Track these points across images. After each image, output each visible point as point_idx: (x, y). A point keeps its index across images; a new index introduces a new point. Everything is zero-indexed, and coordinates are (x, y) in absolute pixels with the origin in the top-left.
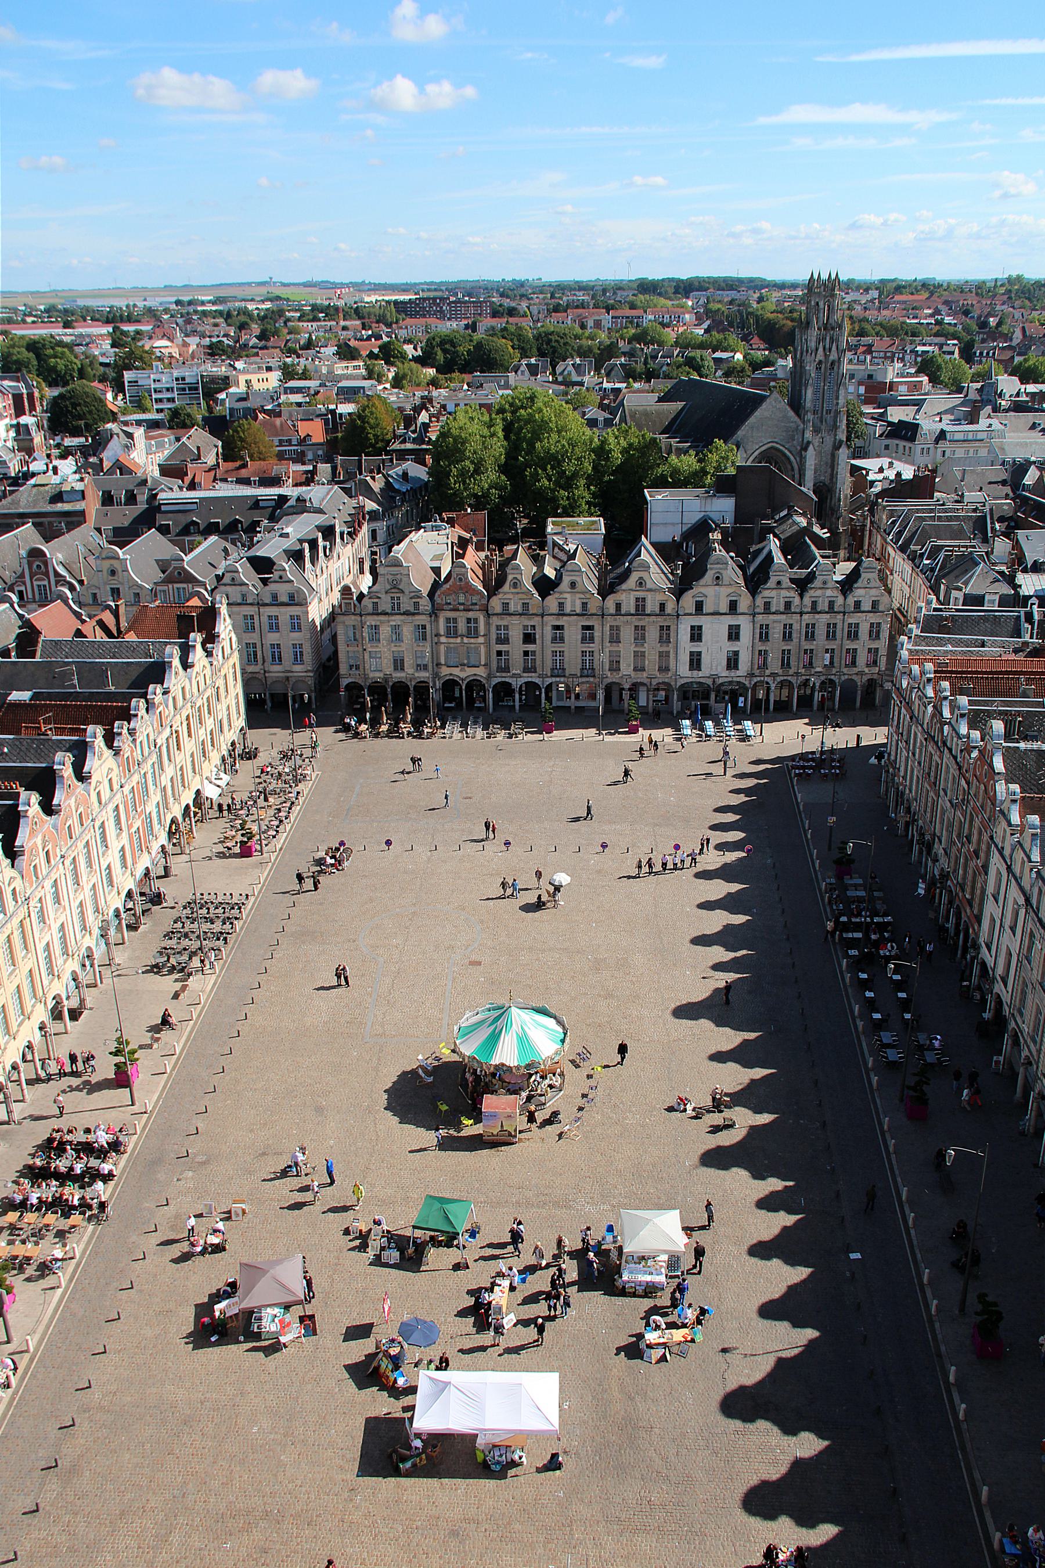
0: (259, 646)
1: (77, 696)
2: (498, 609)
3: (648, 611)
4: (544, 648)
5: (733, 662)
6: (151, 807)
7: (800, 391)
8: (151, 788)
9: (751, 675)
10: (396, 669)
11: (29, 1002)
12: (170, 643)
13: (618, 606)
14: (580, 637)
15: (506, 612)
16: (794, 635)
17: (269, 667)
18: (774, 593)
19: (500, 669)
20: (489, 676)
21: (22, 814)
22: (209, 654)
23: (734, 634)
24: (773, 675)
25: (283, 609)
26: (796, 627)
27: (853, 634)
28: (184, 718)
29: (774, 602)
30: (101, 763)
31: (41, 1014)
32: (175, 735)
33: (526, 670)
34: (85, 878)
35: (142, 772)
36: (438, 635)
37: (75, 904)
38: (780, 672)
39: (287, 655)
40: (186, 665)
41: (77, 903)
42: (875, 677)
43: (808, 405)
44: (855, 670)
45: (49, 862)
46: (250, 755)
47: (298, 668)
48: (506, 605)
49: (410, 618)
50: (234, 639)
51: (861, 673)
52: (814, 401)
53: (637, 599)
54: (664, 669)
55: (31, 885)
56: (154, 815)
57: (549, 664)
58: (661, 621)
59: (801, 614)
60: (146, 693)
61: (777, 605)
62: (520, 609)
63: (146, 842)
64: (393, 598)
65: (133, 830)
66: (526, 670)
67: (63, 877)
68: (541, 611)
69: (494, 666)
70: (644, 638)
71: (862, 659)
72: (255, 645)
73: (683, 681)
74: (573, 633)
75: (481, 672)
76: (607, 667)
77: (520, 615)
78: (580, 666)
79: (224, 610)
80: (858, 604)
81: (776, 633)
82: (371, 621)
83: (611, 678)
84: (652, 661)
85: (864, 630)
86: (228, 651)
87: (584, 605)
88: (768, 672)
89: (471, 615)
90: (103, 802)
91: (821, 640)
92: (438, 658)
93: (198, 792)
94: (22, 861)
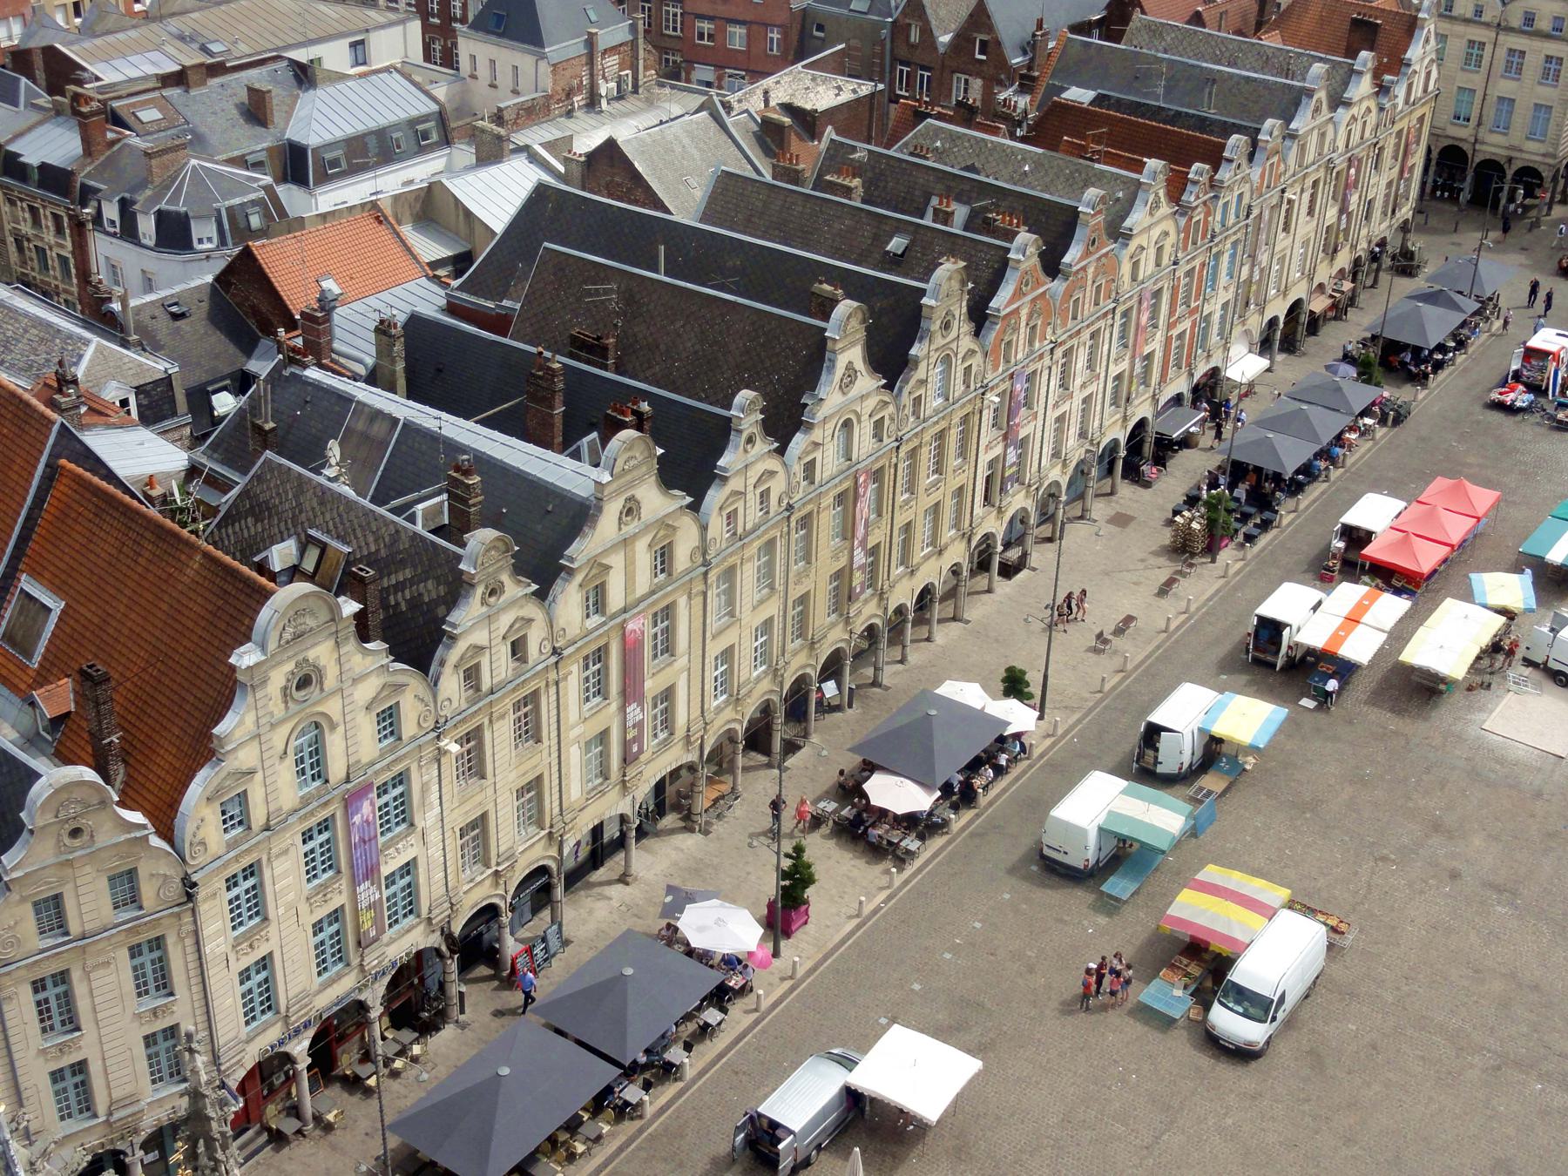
0: (1479, 94)
1: (1155, 113)
6: (1214, 308)
8: (1223, 279)
11: (948, 534)
12: (1321, 60)
17: (1483, 134)
21: (1011, 263)
22: (1382, 90)
25: (1537, 44)
28: (1309, 182)
30: (1152, 222)
31: (958, 553)
32: (1285, 207)
34: (1078, 382)
35: (1214, 250)
37: (1052, 415)
40: (1338, 101)
41: (1058, 413)
45: (1031, 343)
46: (1406, 265)
47: (1531, 146)
50: (1434, 75)
55: (995, 368)
56: (1216, 318)
60: (1258, 131)
63: (1189, 356)
65: (1175, 332)
67: (1046, 373)
79: (1430, 27)
86: (1417, 91)
90: (1141, 277)
93: (1296, 306)
94: (991, 335)
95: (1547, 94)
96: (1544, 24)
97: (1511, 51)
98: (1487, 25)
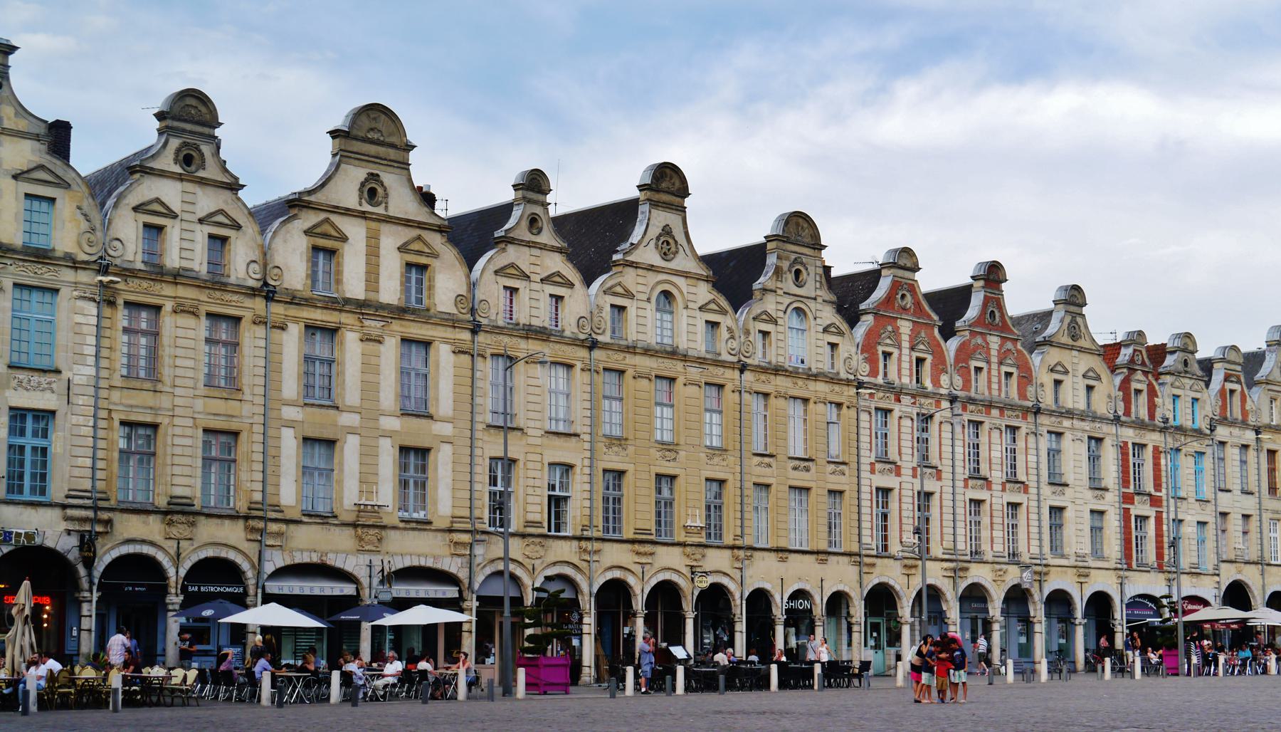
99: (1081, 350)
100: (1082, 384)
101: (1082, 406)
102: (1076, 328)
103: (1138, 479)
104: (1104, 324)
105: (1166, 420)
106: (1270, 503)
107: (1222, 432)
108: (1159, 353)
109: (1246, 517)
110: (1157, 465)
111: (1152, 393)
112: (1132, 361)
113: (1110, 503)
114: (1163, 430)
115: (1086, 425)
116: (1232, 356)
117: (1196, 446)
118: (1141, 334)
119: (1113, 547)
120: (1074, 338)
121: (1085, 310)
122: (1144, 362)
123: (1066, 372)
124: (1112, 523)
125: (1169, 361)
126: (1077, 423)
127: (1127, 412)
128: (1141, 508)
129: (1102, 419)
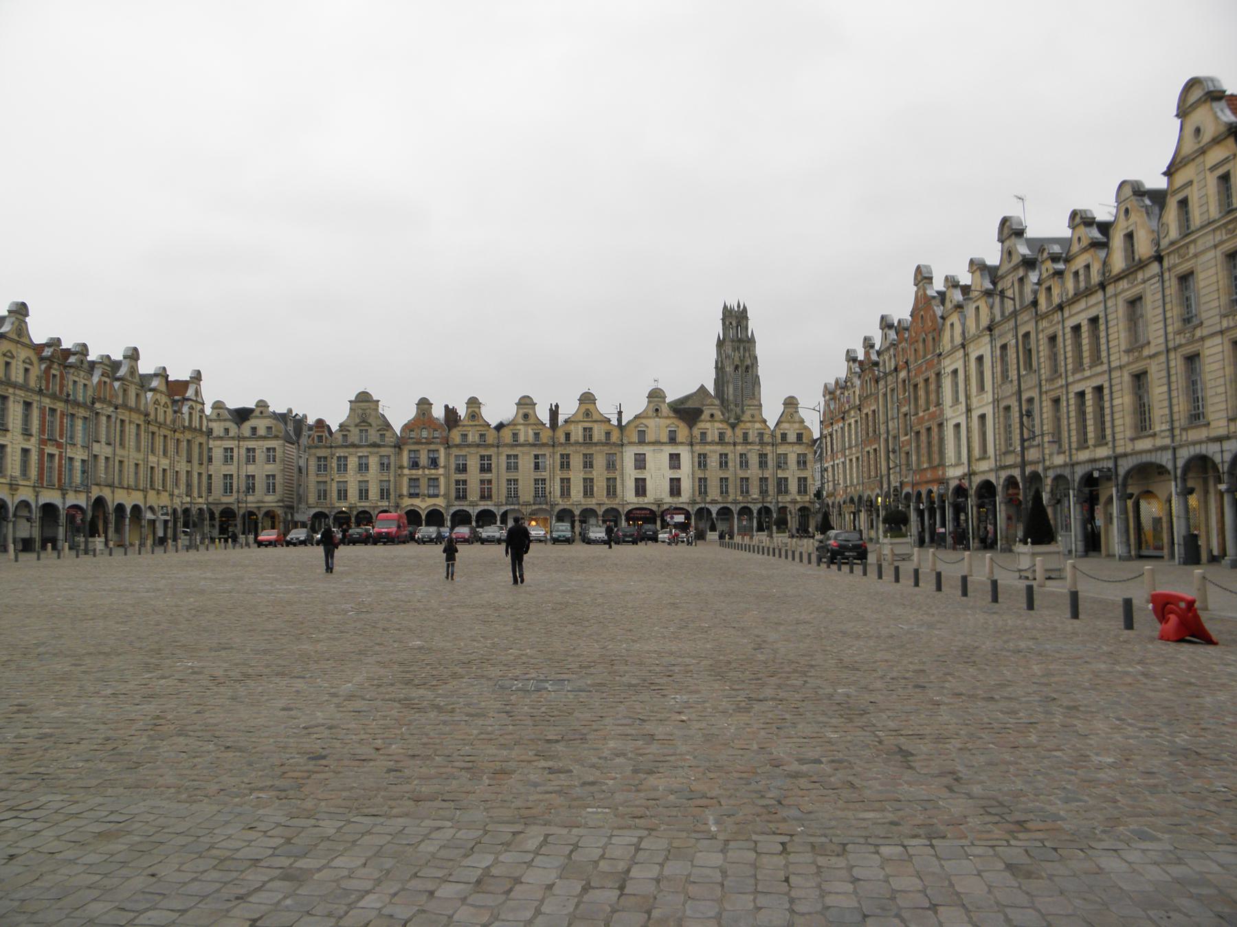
2: (458, 440)
3: (595, 439)
4: (499, 475)
5: (675, 487)
7: (723, 391)
9: (694, 502)
10: (361, 498)
13: (568, 436)
14: (532, 465)
15: (464, 444)
16: (730, 464)
18: (708, 425)
19: (458, 498)
20: (449, 506)
23: (675, 459)
24: (714, 502)
25: (260, 443)
26: (730, 456)
27: (781, 463)
29: (709, 433)
33: (483, 497)
36: (401, 467)
38: (720, 499)
39: (260, 484)
42: (807, 505)
43: (731, 398)
44: (788, 498)
47: (269, 498)
48: (465, 436)
49: (376, 450)
51: (794, 502)
52: (735, 396)
53: (585, 429)
54: (611, 491)
57: (504, 491)
58: (606, 449)
59: (735, 444)
61: (713, 435)
62: (477, 439)
64: (361, 431)
66: (483, 497)
68: (496, 442)
69: (453, 494)
70: (591, 466)
71: (793, 487)
72: (231, 476)
73: (630, 507)
74: (526, 462)
75: (440, 503)
76: (558, 493)
77: (478, 446)
78: (533, 493)
80: (784, 436)
81: (713, 461)
82: (340, 452)
83: (562, 504)
84: (600, 486)
85: (792, 459)
87: (537, 435)
88: (708, 499)
89: (432, 447)
91: (754, 472)
92: (401, 489)
95: (270, 468)
96: (262, 431)
97: (248, 450)
98: (233, 438)
99: (24, 345)
100: (21, 367)
101: (20, 380)
102: (21, 330)
103: (52, 431)
104: (39, 332)
105: (68, 395)
106: (119, 451)
107: (98, 405)
108: (68, 353)
109: (107, 458)
110: (61, 422)
111: (62, 378)
112: (52, 355)
113: (32, 444)
114: (67, 401)
115: (21, 393)
116: (106, 361)
117: (82, 412)
118: (59, 340)
119: (33, 472)
120: (19, 335)
121: (27, 319)
122: (60, 359)
123: (13, 357)
124: (34, 457)
125: (72, 359)
126: (18, 392)
127: (47, 388)
128: (50, 449)
129: (32, 391)
